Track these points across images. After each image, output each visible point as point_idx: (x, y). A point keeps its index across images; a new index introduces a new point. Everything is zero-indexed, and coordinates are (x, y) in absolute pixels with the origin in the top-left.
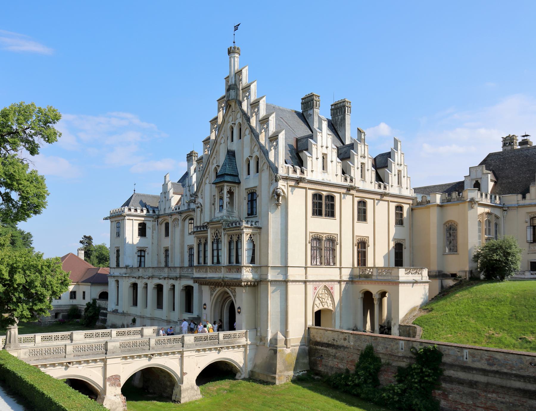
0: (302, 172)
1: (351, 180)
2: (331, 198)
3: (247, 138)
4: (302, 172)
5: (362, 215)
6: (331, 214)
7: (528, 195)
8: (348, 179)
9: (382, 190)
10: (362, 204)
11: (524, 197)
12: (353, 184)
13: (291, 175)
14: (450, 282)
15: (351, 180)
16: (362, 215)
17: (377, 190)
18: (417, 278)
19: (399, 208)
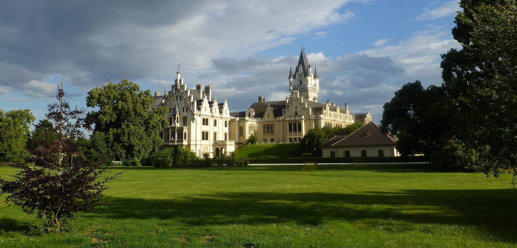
2: (207, 120)
3: (183, 101)
5: (215, 125)
6: (207, 124)
7: (263, 118)
8: (212, 113)
9: (221, 116)
10: (215, 121)
11: (262, 119)
12: (213, 115)
13: (198, 113)
14: (241, 145)
16: (215, 125)
17: (220, 116)
18: (231, 143)
19: (226, 122)
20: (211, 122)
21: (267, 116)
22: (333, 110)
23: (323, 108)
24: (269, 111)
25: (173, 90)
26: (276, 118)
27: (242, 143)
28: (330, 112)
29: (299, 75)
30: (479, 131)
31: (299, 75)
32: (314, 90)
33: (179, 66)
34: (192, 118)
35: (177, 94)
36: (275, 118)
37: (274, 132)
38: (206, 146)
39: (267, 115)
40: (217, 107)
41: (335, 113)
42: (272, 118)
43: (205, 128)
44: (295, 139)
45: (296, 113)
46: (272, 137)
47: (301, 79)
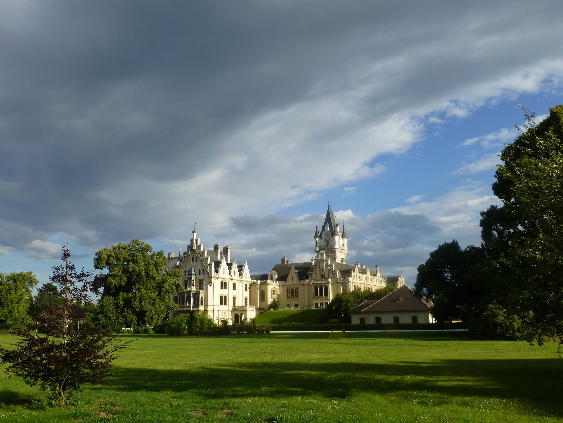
0: (218, 275)
1: (232, 277)
2: (225, 283)
3: (199, 263)
4: (218, 275)
5: (234, 288)
6: (225, 288)
7: (286, 282)
8: (231, 276)
9: (241, 279)
10: (234, 285)
11: (285, 282)
13: (215, 276)
14: (263, 311)
15: (232, 277)
16: (234, 288)
17: (239, 279)
18: (252, 309)
19: (246, 285)
20: (230, 285)
21: (290, 279)
22: (363, 273)
23: (352, 270)
24: (293, 273)
25: (188, 250)
26: (301, 281)
27: (264, 309)
28: (360, 274)
29: (325, 234)
30: (522, 295)
31: (325, 234)
32: (342, 251)
33: (195, 225)
34: (209, 281)
35: (192, 254)
36: (300, 282)
37: (298, 297)
38: (225, 312)
39: (291, 278)
40: (237, 269)
41: (365, 276)
42: (296, 281)
43: (224, 292)
44: (321, 304)
45: (323, 276)
46: (297, 302)
47: (328, 238)
